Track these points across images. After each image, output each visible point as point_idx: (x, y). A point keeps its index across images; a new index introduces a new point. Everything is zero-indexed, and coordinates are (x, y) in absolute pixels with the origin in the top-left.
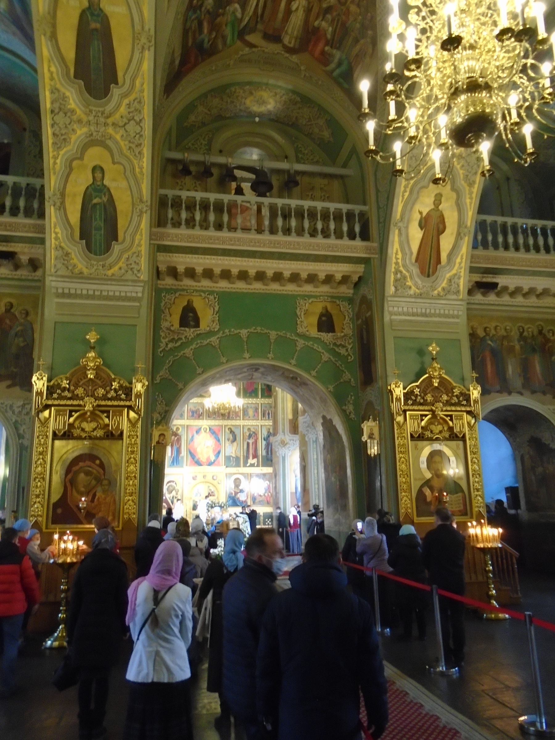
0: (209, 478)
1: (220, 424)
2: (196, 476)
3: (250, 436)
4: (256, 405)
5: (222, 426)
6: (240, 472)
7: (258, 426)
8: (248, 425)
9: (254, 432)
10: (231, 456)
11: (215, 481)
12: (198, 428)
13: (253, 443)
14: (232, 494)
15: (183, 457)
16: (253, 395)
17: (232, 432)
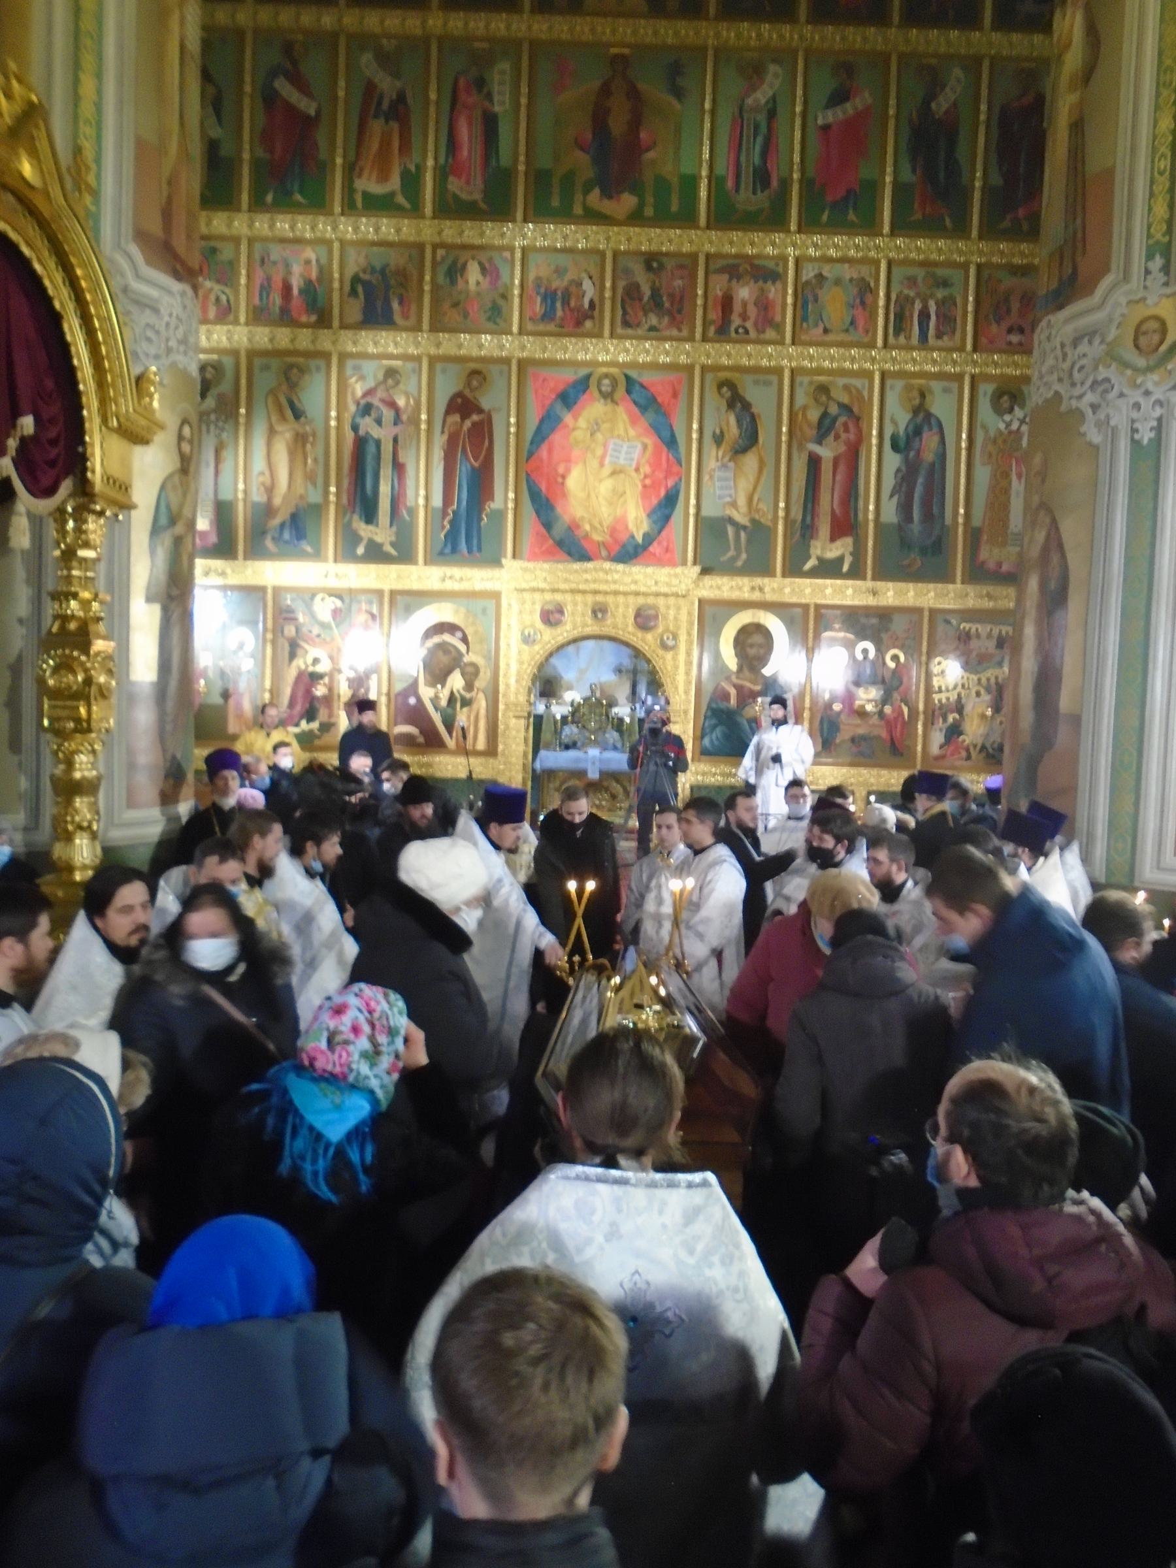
0: (622, 621)
1: (683, 359)
2: (561, 611)
3: (825, 427)
4: (865, 271)
5: (690, 368)
6: (770, 597)
7: (869, 375)
8: (820, 371)
9: (846, 408)
10: (731, 520)
11: (649, 637)
12: (569, 376)
13: (836, 461)
14: (726, 696)
15: (500, 515)
16: (851, 216)
17: (736, 401)
